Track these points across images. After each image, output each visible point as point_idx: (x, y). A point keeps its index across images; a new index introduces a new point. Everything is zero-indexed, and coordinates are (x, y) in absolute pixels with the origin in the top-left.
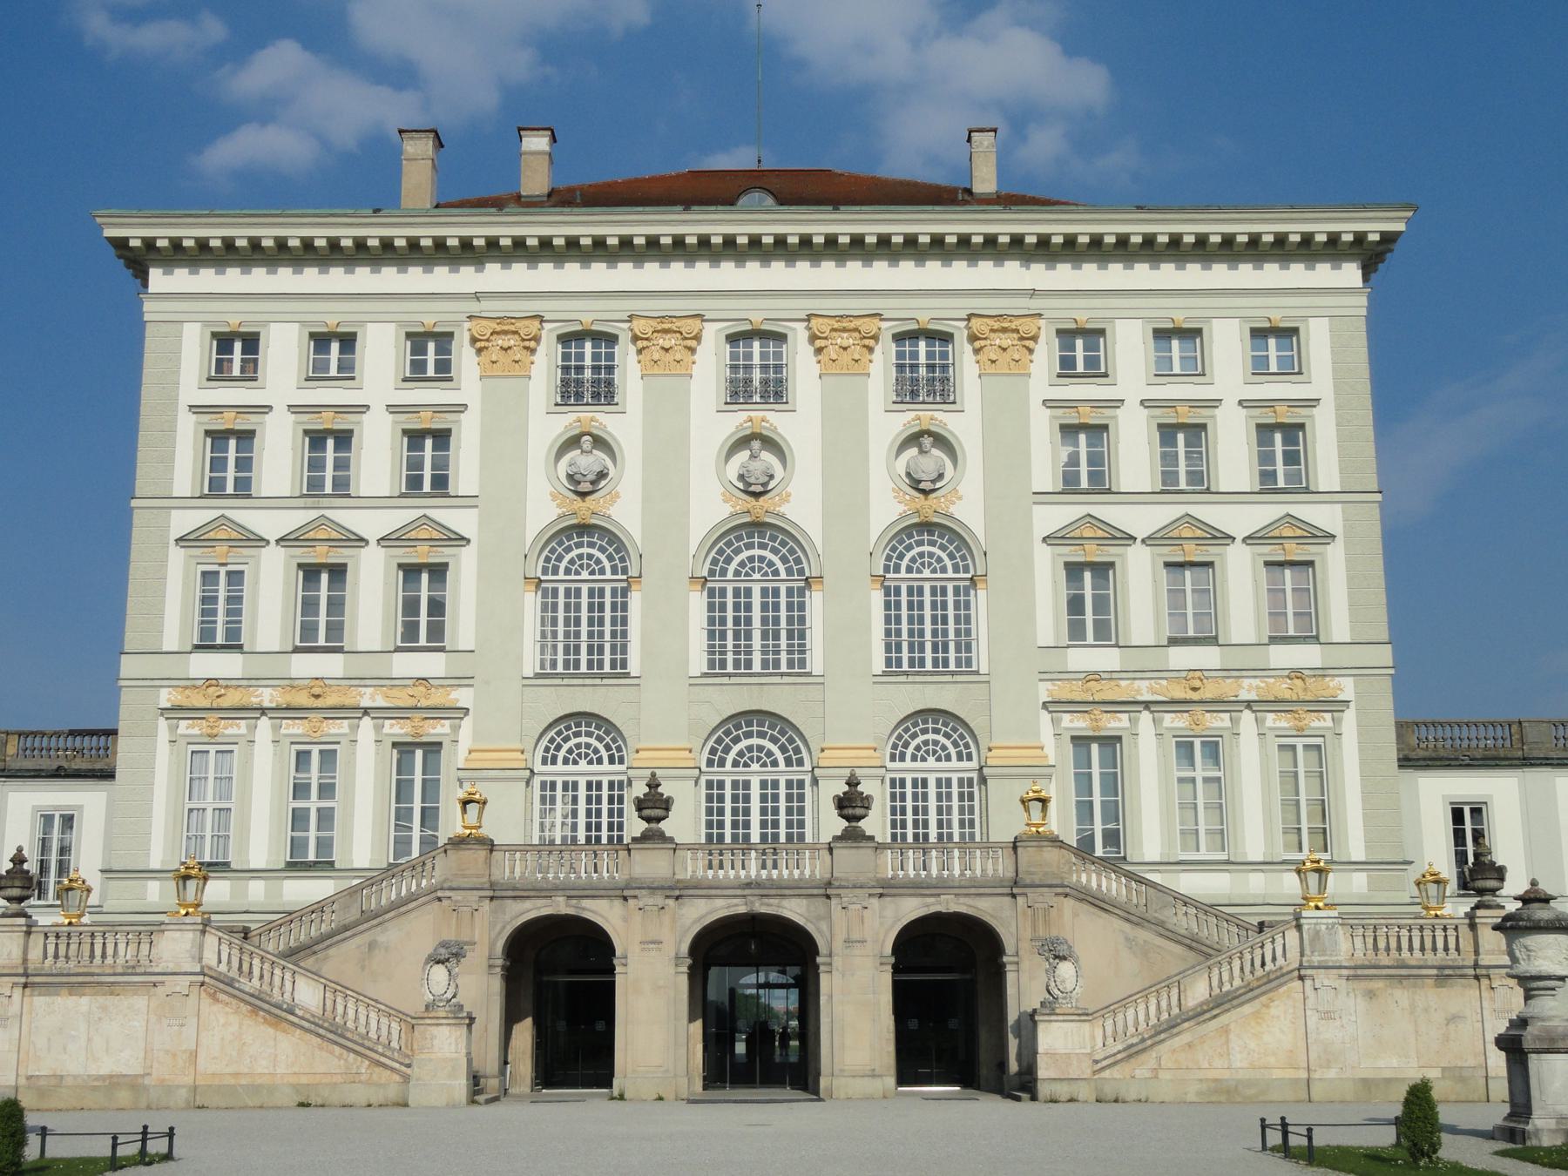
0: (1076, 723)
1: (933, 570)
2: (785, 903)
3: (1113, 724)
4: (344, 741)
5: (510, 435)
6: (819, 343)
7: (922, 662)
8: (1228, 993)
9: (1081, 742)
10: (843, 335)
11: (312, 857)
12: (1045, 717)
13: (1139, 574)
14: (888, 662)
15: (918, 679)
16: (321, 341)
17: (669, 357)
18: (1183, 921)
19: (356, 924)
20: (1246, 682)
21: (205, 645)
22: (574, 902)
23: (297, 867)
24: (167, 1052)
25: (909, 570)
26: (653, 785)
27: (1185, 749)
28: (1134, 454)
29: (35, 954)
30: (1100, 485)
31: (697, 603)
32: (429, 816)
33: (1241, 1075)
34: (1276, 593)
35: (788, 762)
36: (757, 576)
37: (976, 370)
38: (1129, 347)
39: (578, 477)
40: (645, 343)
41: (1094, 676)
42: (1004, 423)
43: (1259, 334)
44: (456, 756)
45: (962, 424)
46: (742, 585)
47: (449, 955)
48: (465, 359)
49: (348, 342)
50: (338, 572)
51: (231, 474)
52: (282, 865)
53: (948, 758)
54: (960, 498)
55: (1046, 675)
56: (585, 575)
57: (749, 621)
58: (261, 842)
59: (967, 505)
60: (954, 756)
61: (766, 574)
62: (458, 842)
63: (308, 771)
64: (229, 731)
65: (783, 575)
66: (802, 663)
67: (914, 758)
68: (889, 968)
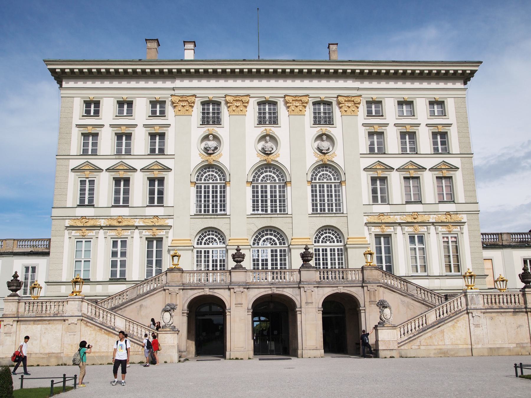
0: (377, 230)
2: (285, 290)
3: (389, 230)
4: (129, 237)
5: (185, 134)
6: (288, 105)
7: (324, 210)
8: (443, 318)
9: (378, 237)
10: (296, 103)
11: (118, 277)
12: (366, 228)
13: (395, 180)
14: (313, 210)
15: (323, 215)
16: (121, 104)
17: (239, 109)
18: (421, 296)
19: (135, 299)
20: (432, 216)
21: (82, 205)
22: (211, 290)
23: (113, 280)
24: (69, 344)
25: (319, 179)
26: (238, 250)
27: (412, 239)
28: (393, 141)
29: (21, 310)
30: (382, 151)
31: (249, 190)
32: (159, 263)
33: (450, 347)
34: (440, 187)
35: (280, 244)
36: (268, 181)
37: (340, 114)
38: (390, 107)
39: (208, 148)
40: (230, 104)
41: (382, 214)
42: (350, 133)
43: (432, 103)
44: (167, 244)
45: (335, 131)
46: (264, 185)
47: (169, 309)
48: (169, 109)
49: (130, 104)
50: (127, 181)
51: (90, 148)
52: (108, 280)
53: (334, 242)
54: (336, 156)
55: (366, 214)
56: (211, 181)
57: (266, 197)
58: (101, 270)
59: (338, 157)
60: (336, 241)
61: (272, 181)
62: (171, 270)
63: (117, 247)
64: (89, 234)
65: (277, 181)
66: (284, 210)
67: (322, 242)
68: (321, 312)
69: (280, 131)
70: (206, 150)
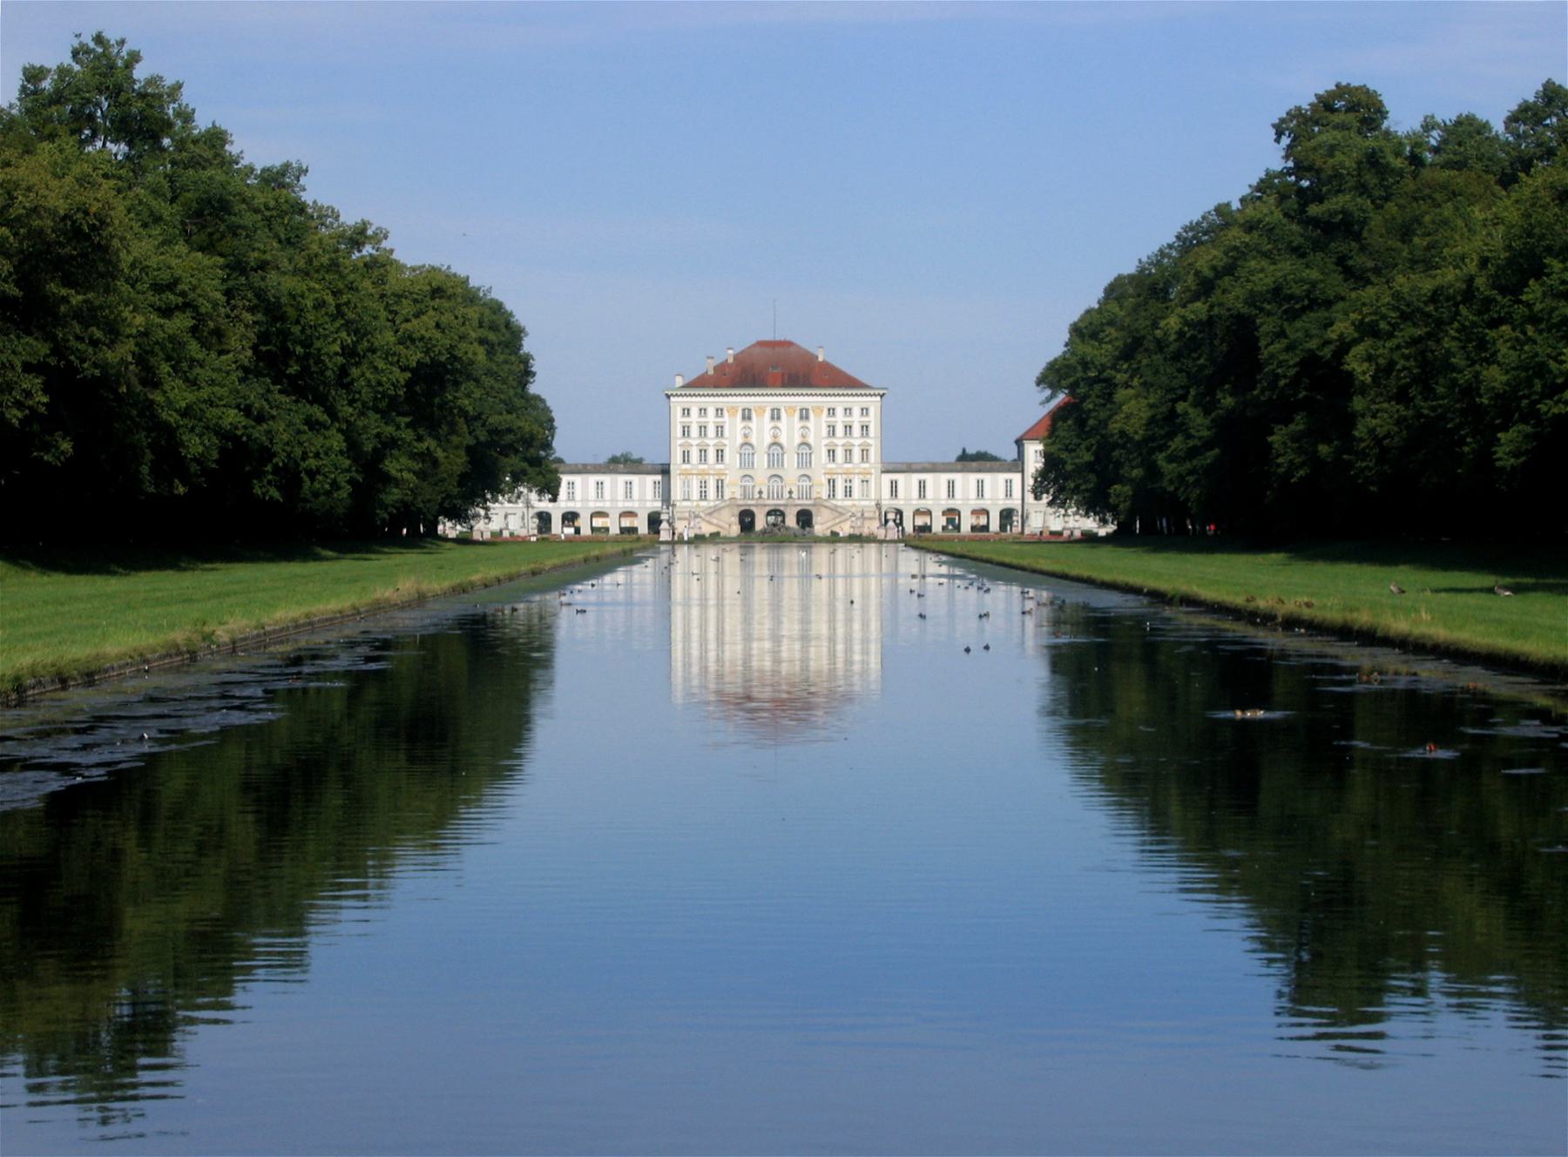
1: (806, 450)
28: (840, 431)
38: (840, 411)
58: (695, 495)
59: (811, 440)
69: (783, 424)
70: (746, 436)
